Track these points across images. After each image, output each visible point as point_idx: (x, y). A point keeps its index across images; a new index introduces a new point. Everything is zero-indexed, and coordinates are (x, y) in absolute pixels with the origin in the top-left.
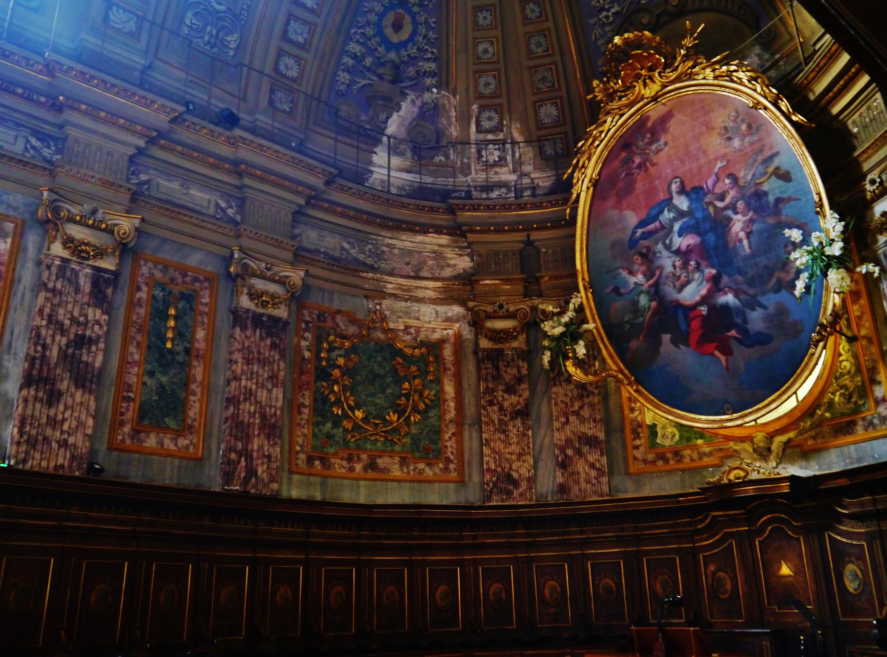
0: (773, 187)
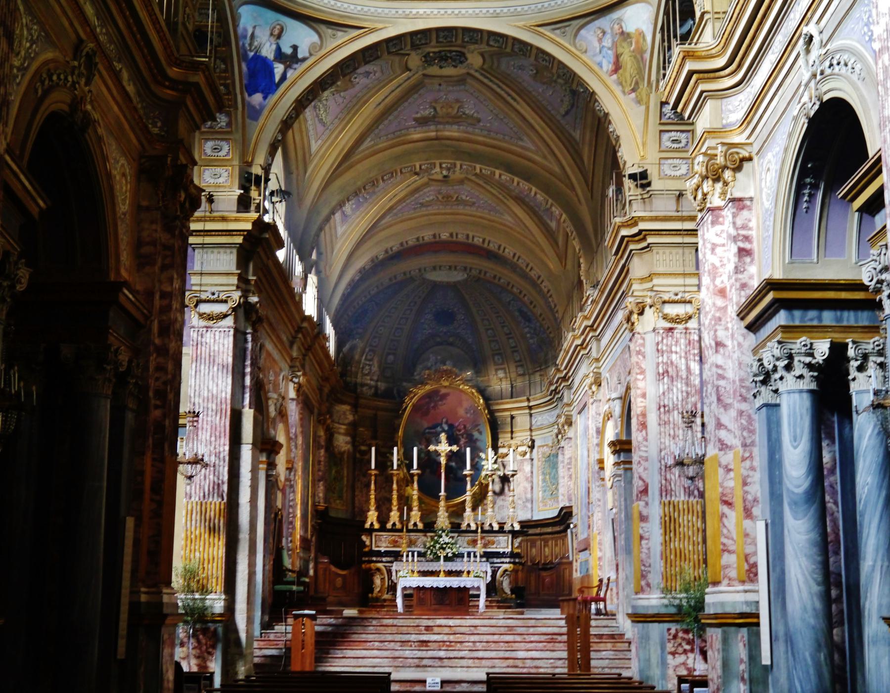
0: (476, 435)
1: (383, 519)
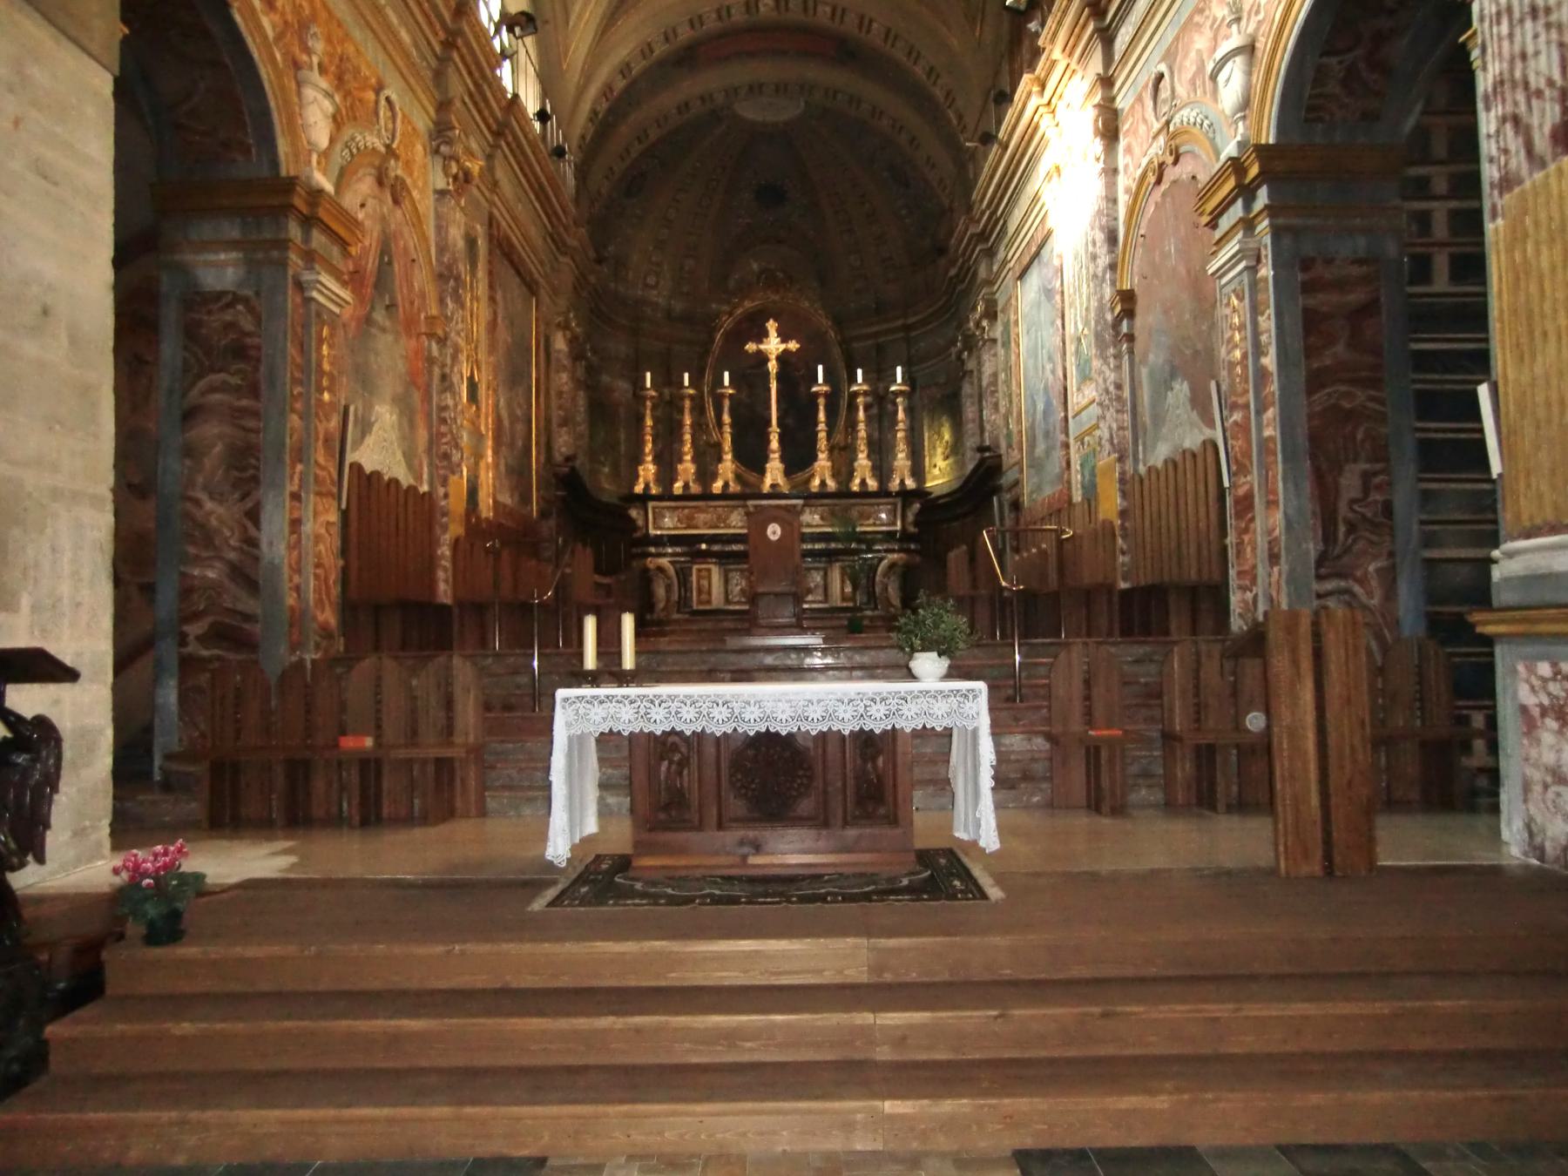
1: (667, 473)
